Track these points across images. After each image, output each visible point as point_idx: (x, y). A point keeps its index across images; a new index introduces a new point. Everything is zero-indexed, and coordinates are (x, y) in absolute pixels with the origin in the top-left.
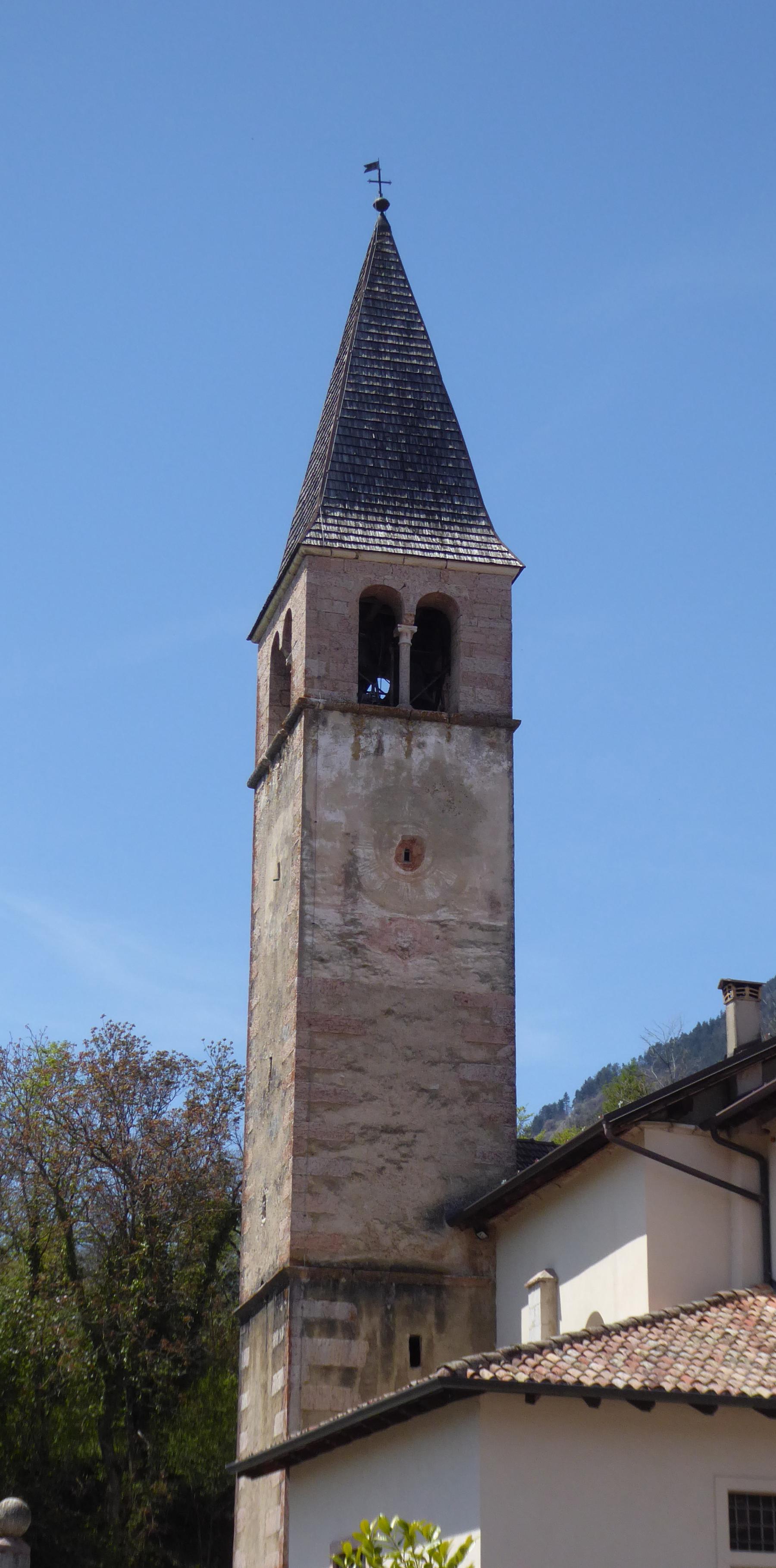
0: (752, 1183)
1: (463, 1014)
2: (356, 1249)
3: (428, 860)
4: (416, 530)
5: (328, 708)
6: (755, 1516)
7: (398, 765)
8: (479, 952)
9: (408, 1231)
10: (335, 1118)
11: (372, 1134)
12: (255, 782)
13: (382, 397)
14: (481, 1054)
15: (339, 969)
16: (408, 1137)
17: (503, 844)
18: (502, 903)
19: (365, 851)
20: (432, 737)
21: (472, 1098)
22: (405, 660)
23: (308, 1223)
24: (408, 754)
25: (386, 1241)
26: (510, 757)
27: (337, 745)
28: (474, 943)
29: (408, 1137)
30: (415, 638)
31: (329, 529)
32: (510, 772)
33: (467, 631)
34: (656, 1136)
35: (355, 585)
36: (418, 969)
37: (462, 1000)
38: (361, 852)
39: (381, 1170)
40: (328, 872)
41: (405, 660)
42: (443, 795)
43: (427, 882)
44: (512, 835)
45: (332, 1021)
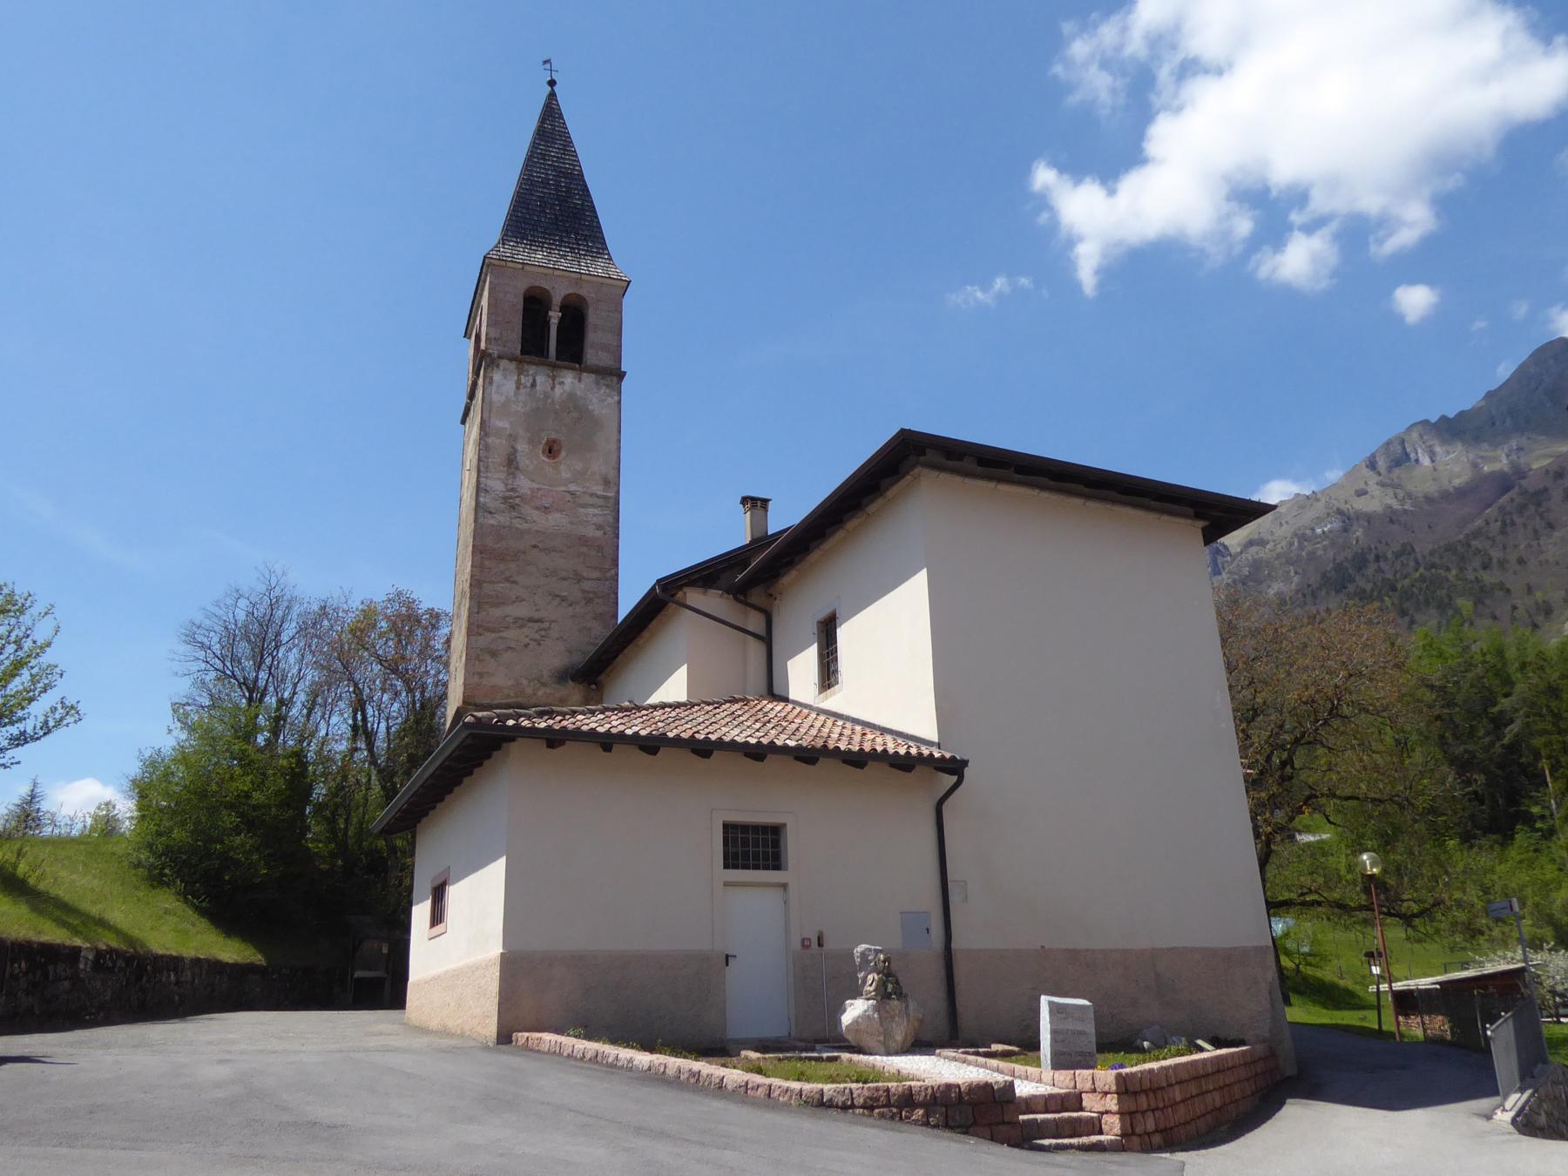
0: (762, 631)
1: (585, 549)
2: (509, 696)
3: (563, 454)
4: (563, 257)
5: (500, 357)
6: (745, 843)
7: (546, 396)
8: (596, 511)
9: (544, 685)
10: (497, 612)
11: (521, 623)
12: (463, 422)
13: (545, 183)
14: (596, 574)
15: (503, 519)
16: (546, 625)
17: (614, 447)
18: (612, 482)
19: (522, 447)
20: (568, 379)
21: (589, 601)
22: (551, 330)
23: (476, 679)
24: (553, 388)
25: (529, 691)
26: (620, 393)
27: (504, 382)
28: (593, 506)
29: (546, 625)
30: (561, 320)
31: (506, 251)
32: (619, 402)
33: (592, 318)
34: (694, 597)
35: (522, 285)
36: (556, 520)
37: (584, 541)
38: (519, 447)
39: (526, 646)
40: (497, 459)
41: (551, 330)
42: (575, 415)
43: (562, 467)
44: (619, 441)
45: (494, 555)
